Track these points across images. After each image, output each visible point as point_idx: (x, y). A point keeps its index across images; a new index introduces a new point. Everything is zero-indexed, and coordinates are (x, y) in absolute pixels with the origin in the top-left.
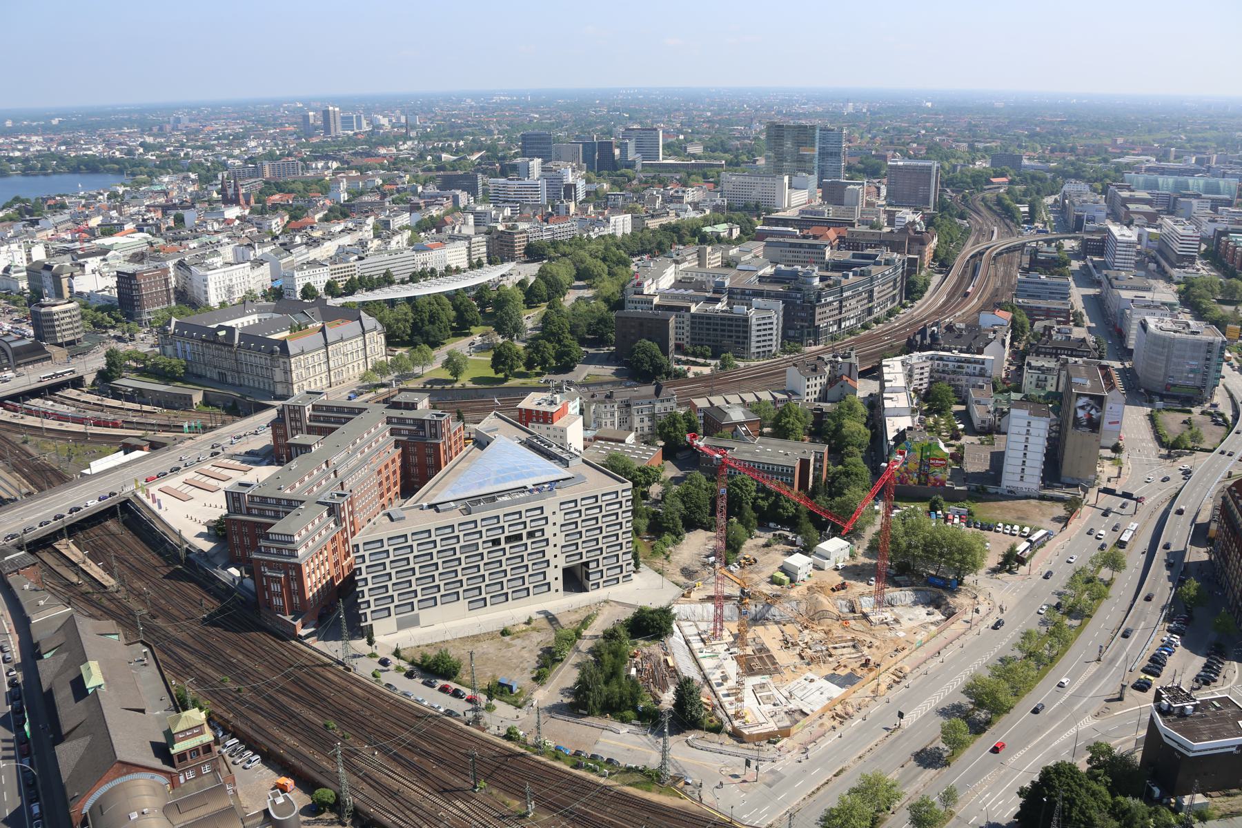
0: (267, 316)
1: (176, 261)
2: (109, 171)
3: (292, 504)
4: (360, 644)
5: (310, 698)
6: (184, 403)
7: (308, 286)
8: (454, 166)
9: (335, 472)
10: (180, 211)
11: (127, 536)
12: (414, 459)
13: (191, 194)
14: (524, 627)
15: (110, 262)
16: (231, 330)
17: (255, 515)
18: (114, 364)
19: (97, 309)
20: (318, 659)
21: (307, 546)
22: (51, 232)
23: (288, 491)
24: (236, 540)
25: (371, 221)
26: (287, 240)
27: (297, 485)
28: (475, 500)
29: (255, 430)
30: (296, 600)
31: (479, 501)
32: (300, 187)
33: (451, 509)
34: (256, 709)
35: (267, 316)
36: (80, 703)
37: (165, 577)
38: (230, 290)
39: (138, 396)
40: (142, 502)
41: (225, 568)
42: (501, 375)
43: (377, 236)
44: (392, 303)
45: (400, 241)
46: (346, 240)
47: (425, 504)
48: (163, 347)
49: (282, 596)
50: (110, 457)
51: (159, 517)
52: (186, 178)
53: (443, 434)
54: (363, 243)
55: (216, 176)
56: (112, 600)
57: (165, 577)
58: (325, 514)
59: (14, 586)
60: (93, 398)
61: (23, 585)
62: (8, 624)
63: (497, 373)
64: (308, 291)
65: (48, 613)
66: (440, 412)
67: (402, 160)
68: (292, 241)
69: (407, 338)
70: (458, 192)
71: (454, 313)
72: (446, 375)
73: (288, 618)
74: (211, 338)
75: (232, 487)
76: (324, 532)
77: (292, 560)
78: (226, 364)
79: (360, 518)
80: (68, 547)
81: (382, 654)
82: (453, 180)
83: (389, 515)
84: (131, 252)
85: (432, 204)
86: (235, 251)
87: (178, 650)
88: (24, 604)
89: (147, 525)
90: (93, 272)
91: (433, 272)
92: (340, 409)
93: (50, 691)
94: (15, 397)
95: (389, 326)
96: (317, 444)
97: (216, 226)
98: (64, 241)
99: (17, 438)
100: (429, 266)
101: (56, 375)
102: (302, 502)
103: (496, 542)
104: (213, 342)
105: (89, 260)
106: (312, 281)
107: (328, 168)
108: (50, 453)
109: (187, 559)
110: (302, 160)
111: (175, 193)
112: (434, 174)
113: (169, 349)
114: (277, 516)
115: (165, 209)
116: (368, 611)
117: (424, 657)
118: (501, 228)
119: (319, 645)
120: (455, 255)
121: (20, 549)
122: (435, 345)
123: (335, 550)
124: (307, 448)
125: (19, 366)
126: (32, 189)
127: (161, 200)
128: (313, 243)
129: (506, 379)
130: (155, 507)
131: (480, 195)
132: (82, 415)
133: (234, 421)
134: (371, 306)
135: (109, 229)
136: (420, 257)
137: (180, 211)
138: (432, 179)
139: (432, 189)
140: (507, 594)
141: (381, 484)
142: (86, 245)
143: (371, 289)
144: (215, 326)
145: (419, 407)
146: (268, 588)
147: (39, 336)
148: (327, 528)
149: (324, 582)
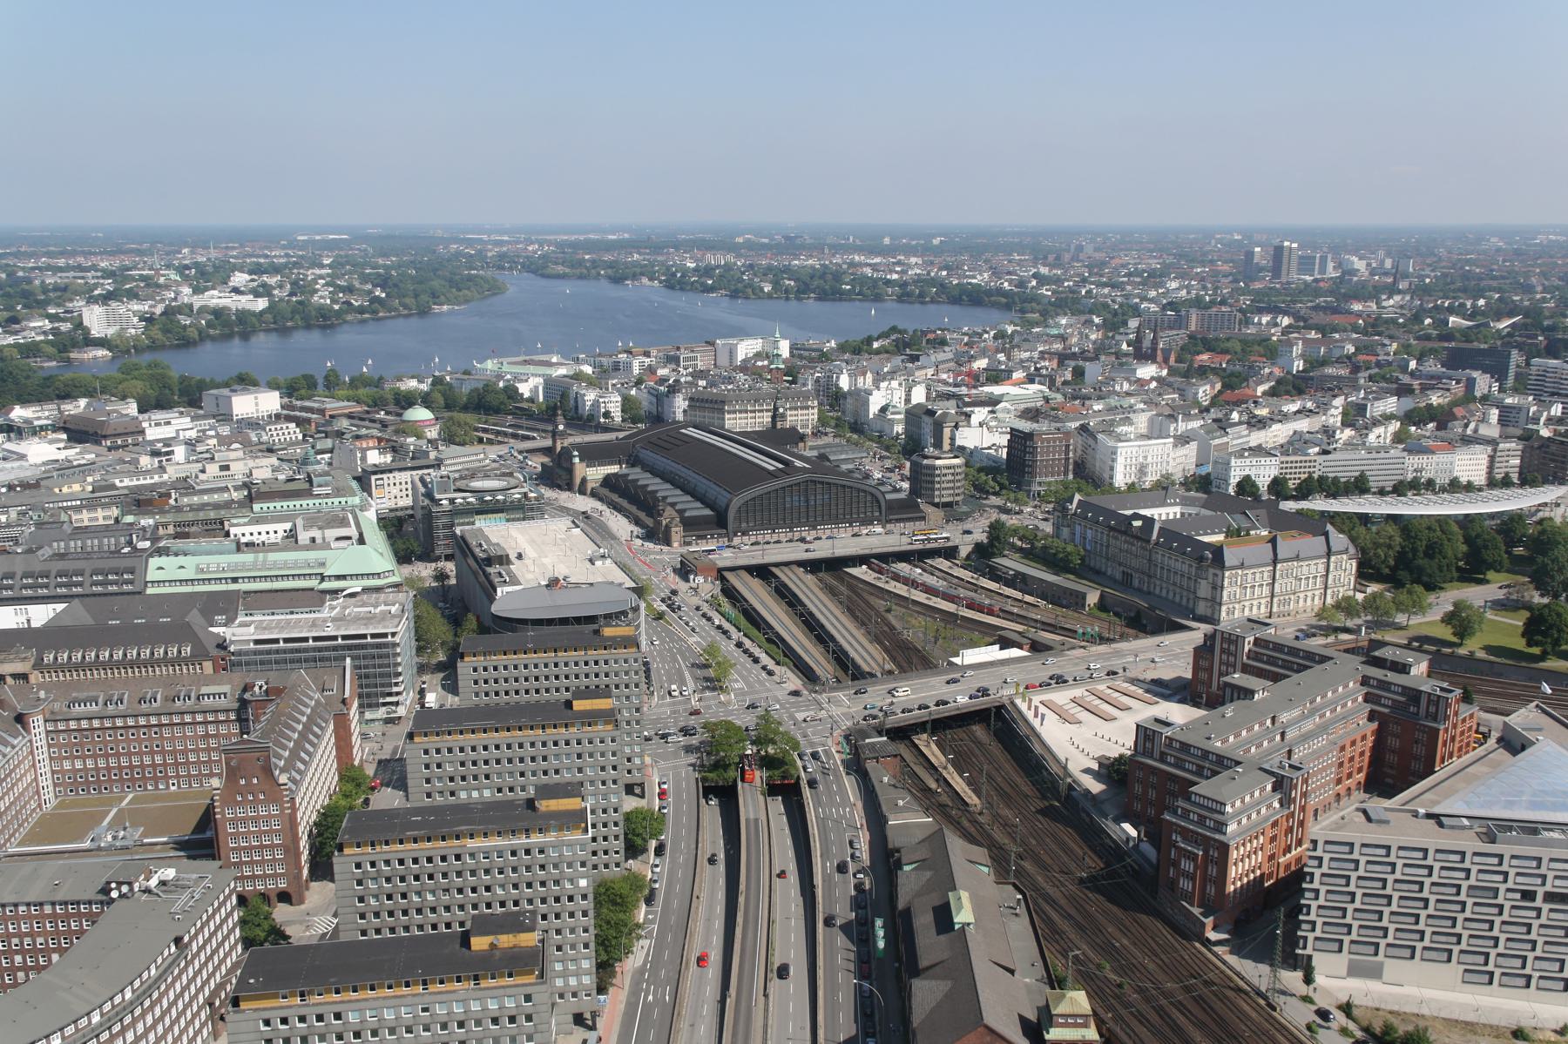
0: (1193, 510)
1: (1077, 424)
2: (995, 305)
3: (1221, 764)
4: (1292, 979)
5: (1213, 1026)
6: (1077, 601)
7: (1247, 479)
8: (1466, 334)
9: (1283, 735)
10: (1081, 363)
11: (995, 748)
12: (1394, 742)
13: (1094, 342)
14: (1553, 1037)
15: (999, 415)
16: (1149, 522)
17: (1169, 764)
18: (997, 538)
19: (980, 470)
20: (1230, 979)
21: (1239, 823)
22: (930, 372)
23: (1219, 744)
24: (1138, 789)
25: (1339, 402)
26: (1220, 415)
27: (1231, 739)
28: (1506, 825)
29: (1172, 654)
30: (1211, 890)
31: (1510, 829)
32: (1238, 348)
33: (1463, 828)
34: (1141, 1018)
35: (1193, 510)
36: (942, 937)
37: (1038, 812)
38: (1142, 471)
39: (1020, 581)
40: (1020, 712)
41: (1118, 820)
42: (1536, 650)
43: (1346, 424)
44: (1365, 519)
45: (1380, 435)
46: (1303, 425)
47: (1422, 811)
48: (1057, 527)
49: (1193, 879)
50: (983, 649)
51: (1038, 736)
52: (1089, 323)
53: (1446, 718)
54: (1328, 432)
55: (1125, 323)
56: (974, 822)
57: (1038, 812)
58: (1269, 787)
59: (872, 775)
60: (966, 575)
61: (883, 777)
62: (859, 818)
63: (1529, 645)
64: (1246, 485)
65: (908, 820)
66: (1445, 685)
67: (1387, 321)
68: (1227, 416)
69: (1387, 571)
70: (1475, 374)
71: (1464, 548)
72: (1446, 633)
73: (1196, 911)
74: (1122, 527)
75: (1146, 720)
76: (1263, 811)
77: (1217, 836)
78: (1135, 563)
79: (1313, 802)
80: (928, 746)
81: (1322, 1003)
82: (1461, 356)
83: (1365, 812)
84: (1022, 406)
85: (1432, 388)
86: (1151, 421)
87: (1048, 909)
88: (882, 799)
89: (1022, 742)
90: (981, 425)
91: (1430, 484)
92: (1293, 651)
93: (907, 913)
94: (886, 558)
95: (1363, 551)
96: (1263, 692)
97: (1126, 386)
98: (945, 383)
99: (880, 604)
100: (1425, 476)
101: (929, 540)
102: (1238, 763)
103: (1528, 895)
104: (1125, 533)
105: (976, 409)
106: (1252, 473)
107: (1276, 325)
108: (914, 631)
109: (1068, 796)
110: (1241, 310)
111: (1074, 340)
112: (1436, 345)
113: (1065, 531)
114: (1199, 772)
115: (1063, 358)
116: (1311, 936)
117: (1388, 1029)
118: (1545, 433)
119: (1232, 960)
120: (1470, 465)
121: (880, 734)
122: (1431, 587)
123: (1273, 839)
124: (1248, 693)
125: (889, 521)
126: (912, 319)
127: (1058, 346)
128: (1258, 424)
129: (1542, 657)
130: (1036, 723)
131: (1510, 381)
132: (953, 592)
133: (1136, 637)
134: (1338, 519)
135: (995, 376)
136: (1413, 462)
137: (1081, 363)
138: (1433, 351)
139: (1433, 366)
140: (1529, 978)
141: (1341, 765)
142: (974, 391)
143: (1334, 495)
144: (1129, 512)
145: (1414, 671)
146: (1176, 864)
147: (914, 491)
148: (1270, 806)
149: (1252, 876)
